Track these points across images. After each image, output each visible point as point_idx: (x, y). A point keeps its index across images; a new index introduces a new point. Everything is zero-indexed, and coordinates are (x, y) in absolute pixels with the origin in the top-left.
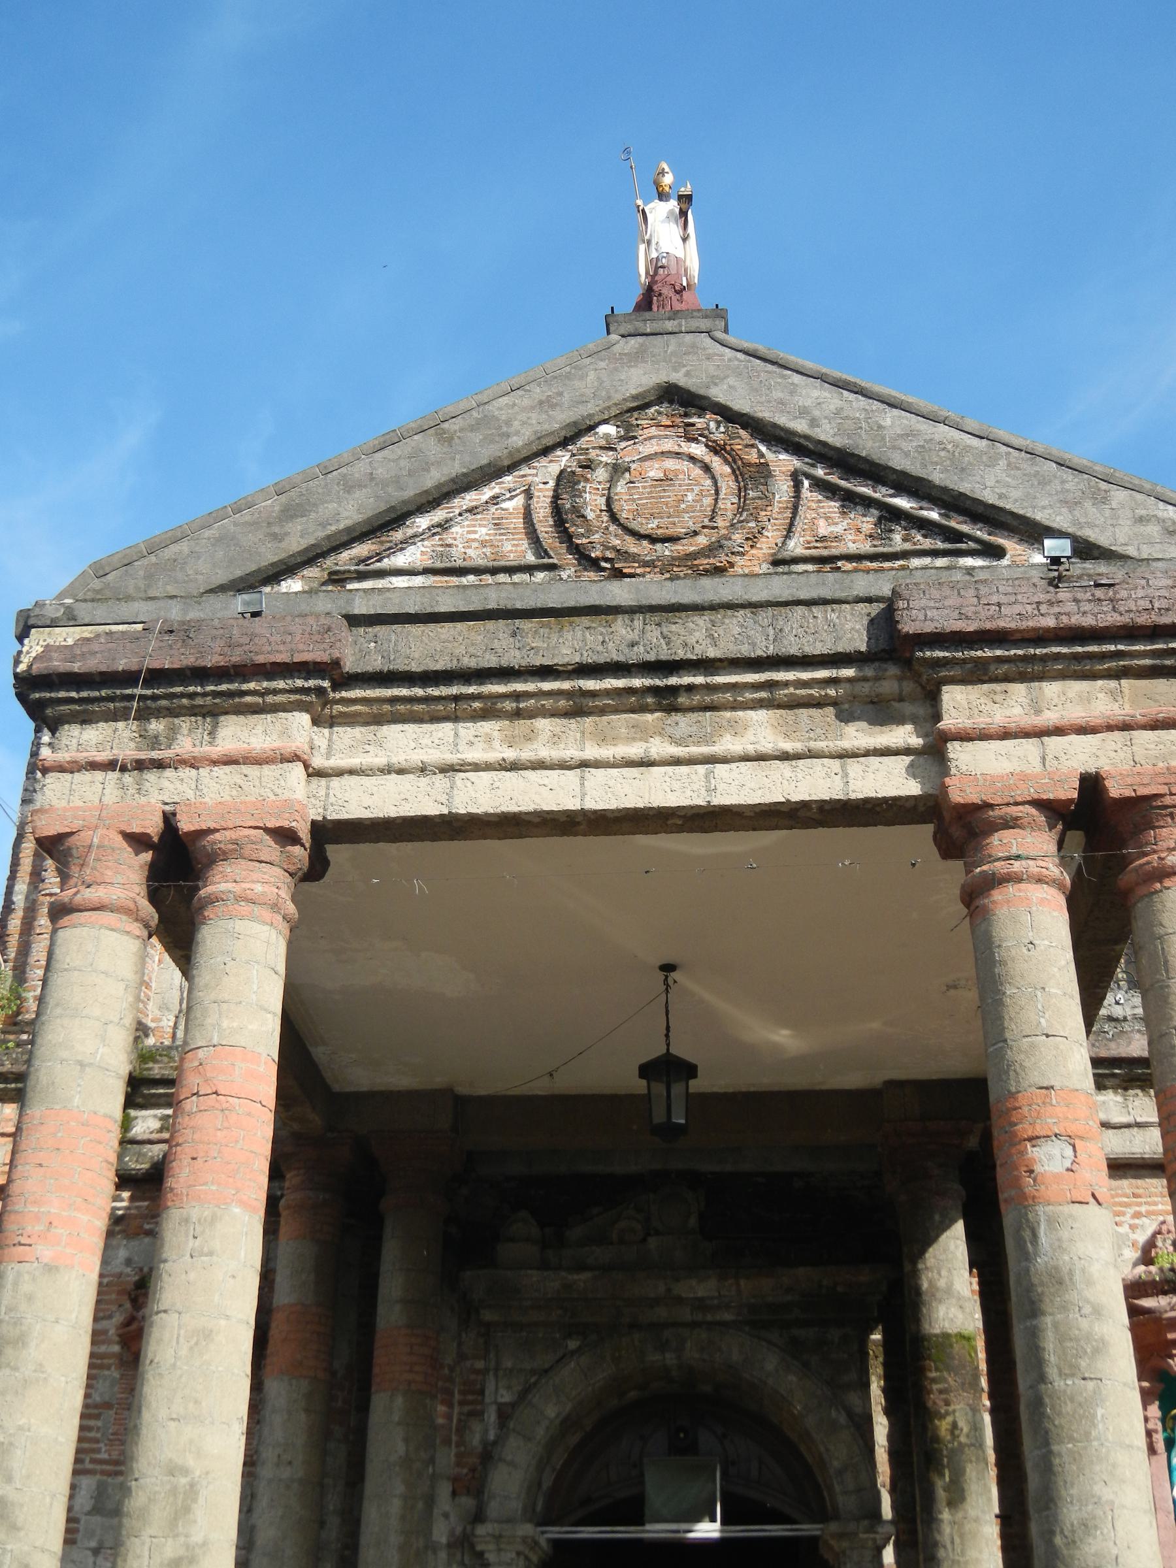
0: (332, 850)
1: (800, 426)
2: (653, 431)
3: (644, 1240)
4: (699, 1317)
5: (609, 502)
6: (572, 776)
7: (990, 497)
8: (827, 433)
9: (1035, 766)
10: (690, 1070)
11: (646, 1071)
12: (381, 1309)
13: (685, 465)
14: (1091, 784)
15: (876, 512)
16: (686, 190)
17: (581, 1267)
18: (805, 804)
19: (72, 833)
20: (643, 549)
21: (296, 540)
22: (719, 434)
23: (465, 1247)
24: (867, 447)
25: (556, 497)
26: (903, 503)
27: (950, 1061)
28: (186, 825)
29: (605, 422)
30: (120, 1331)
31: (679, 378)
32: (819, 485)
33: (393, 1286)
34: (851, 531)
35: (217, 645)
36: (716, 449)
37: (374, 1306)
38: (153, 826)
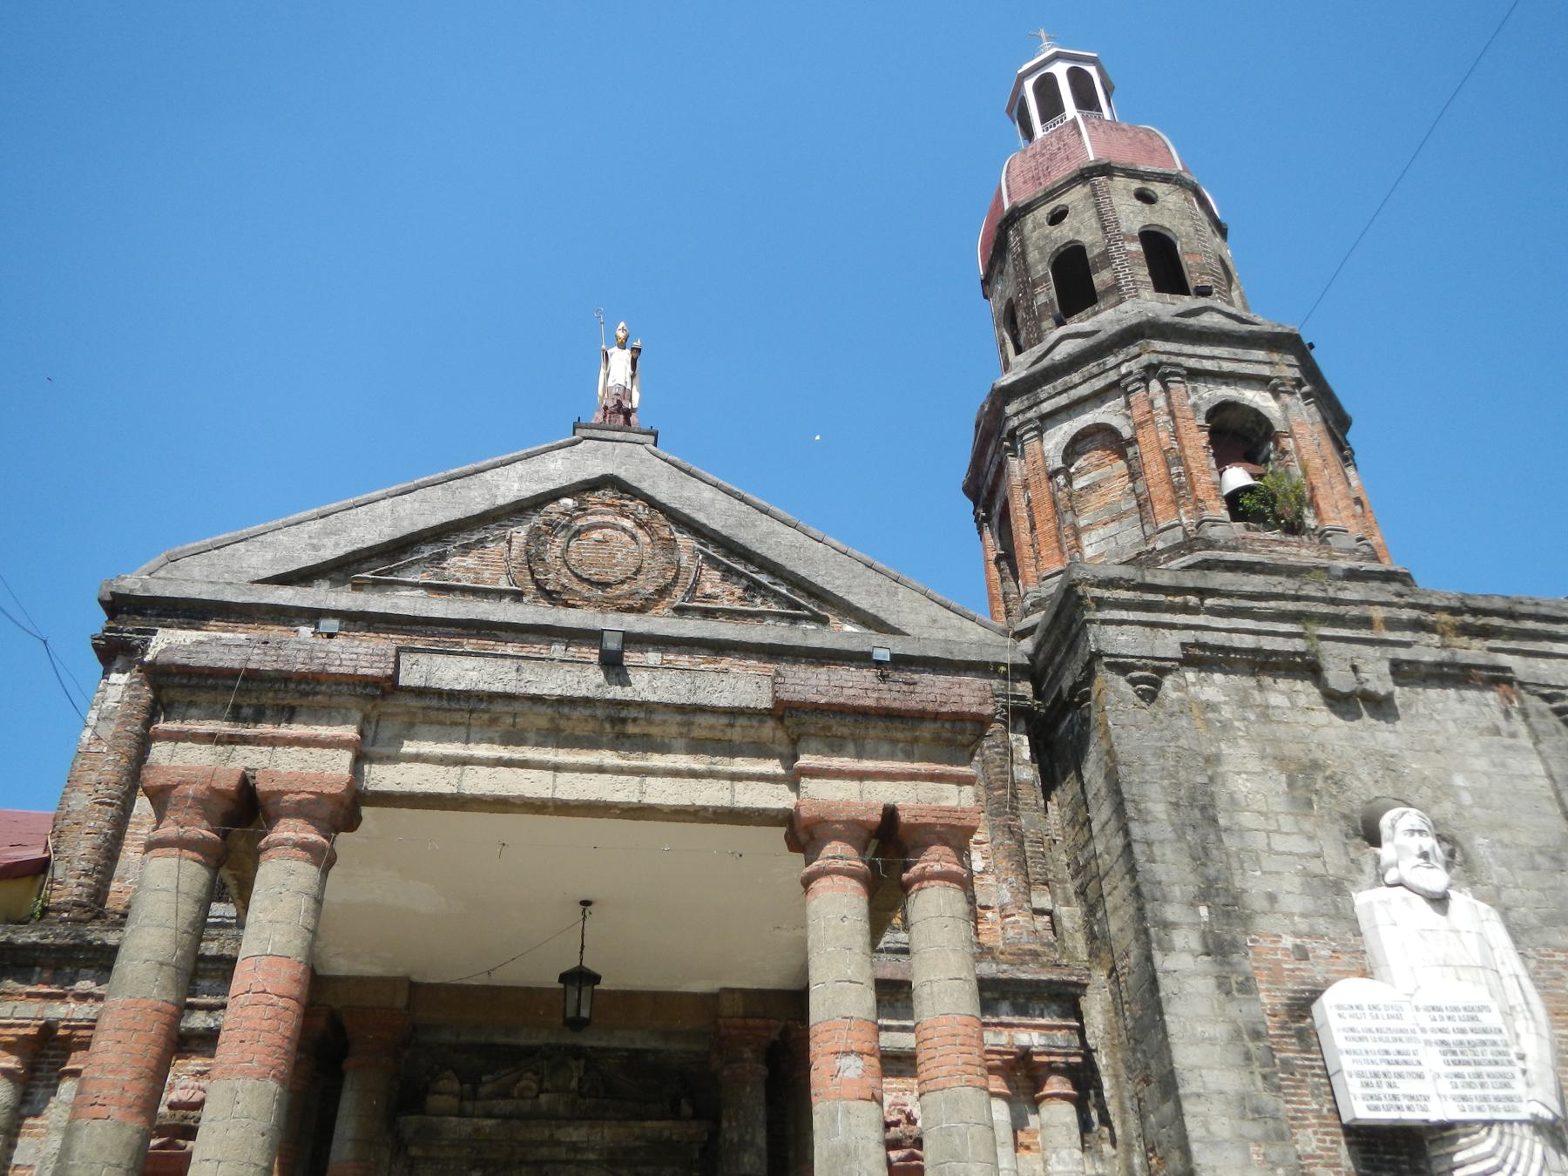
0: (366, 812)
1: (701, 517)
2: (599, 507)
3: (537, 1096)
4: (572, 1156)
6: (549, 775)
7: (819, 581)
8: (716, 524)
9: (855, 799)
10: (596, 979)
11: (564, 978)
12: (335, 1146)
14: (890, 813)
15: (744, 582)
16: (637, 344)
17: (489, 1115)
18: (705, 808)
19: (175, 787)
20: (584, 589)
21: (330, 552)
22: (643, 512)
23: (406, 1096)
24: (744, 537)
26: (764, 579)
27: (769, 976)
28: (262, 786)
29: (567, 496)
31: (622, 473)
32: (708, 558)
33: (347, 1126)
35: (301, 656)
36: (641, 525)
37: (329, 1141)
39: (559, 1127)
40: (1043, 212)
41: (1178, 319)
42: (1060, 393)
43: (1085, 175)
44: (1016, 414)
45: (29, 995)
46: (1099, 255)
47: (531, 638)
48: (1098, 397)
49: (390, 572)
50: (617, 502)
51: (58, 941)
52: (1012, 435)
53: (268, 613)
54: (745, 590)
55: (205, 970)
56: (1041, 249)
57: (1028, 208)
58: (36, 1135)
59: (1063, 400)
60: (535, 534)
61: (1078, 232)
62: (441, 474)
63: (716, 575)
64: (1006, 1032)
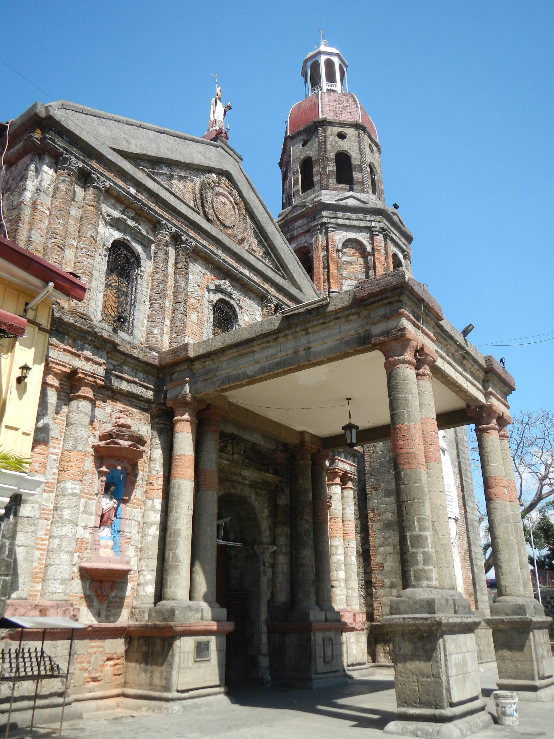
1: (255, 211)
4: (242, 481)
5: (212, 200)
13: (228, 203)
20: (218, 222)
21: (134, 149)
25: (201, 190)
28: (426, 350)
30: (102, 443)
34: (259, 252)
38: (420, 346)
39: (244, 469)
40: (337, 130)
41: (392, 214)
42: (347, 219)
43: (357, 126)
44: (327, 217)
45: (65, 350)
46: (357, 165)
47: (212, 242)
48: (360, 229)
49: (154, 173)
50: (230, 187)
51: (83, 327)
52: (325, 224)
53: (118, 171)
54: (264, 253)
55: (129, 362)
56: (333, 147)
57: (331, 124)
58: (58, 423)
59: (347, 222)
60: (204, 186)
61: (350, 149)
62: (172, 131)
63: (256, 241)
64: (343, 464)
